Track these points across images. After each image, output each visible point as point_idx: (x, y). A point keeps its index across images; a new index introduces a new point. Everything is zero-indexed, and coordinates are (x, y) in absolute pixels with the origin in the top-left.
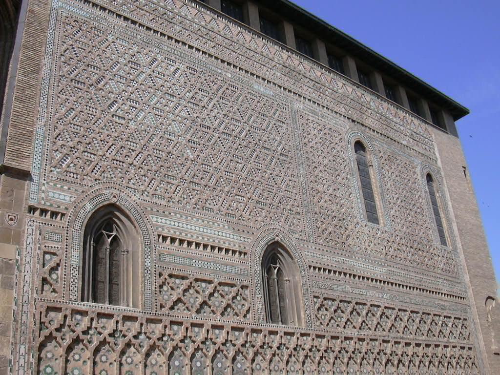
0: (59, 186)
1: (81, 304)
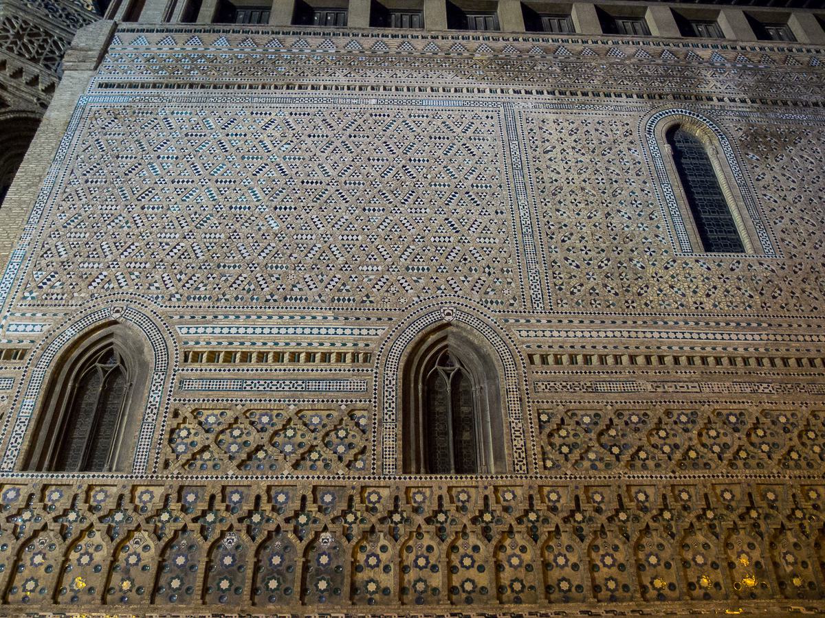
0: (28, 315)
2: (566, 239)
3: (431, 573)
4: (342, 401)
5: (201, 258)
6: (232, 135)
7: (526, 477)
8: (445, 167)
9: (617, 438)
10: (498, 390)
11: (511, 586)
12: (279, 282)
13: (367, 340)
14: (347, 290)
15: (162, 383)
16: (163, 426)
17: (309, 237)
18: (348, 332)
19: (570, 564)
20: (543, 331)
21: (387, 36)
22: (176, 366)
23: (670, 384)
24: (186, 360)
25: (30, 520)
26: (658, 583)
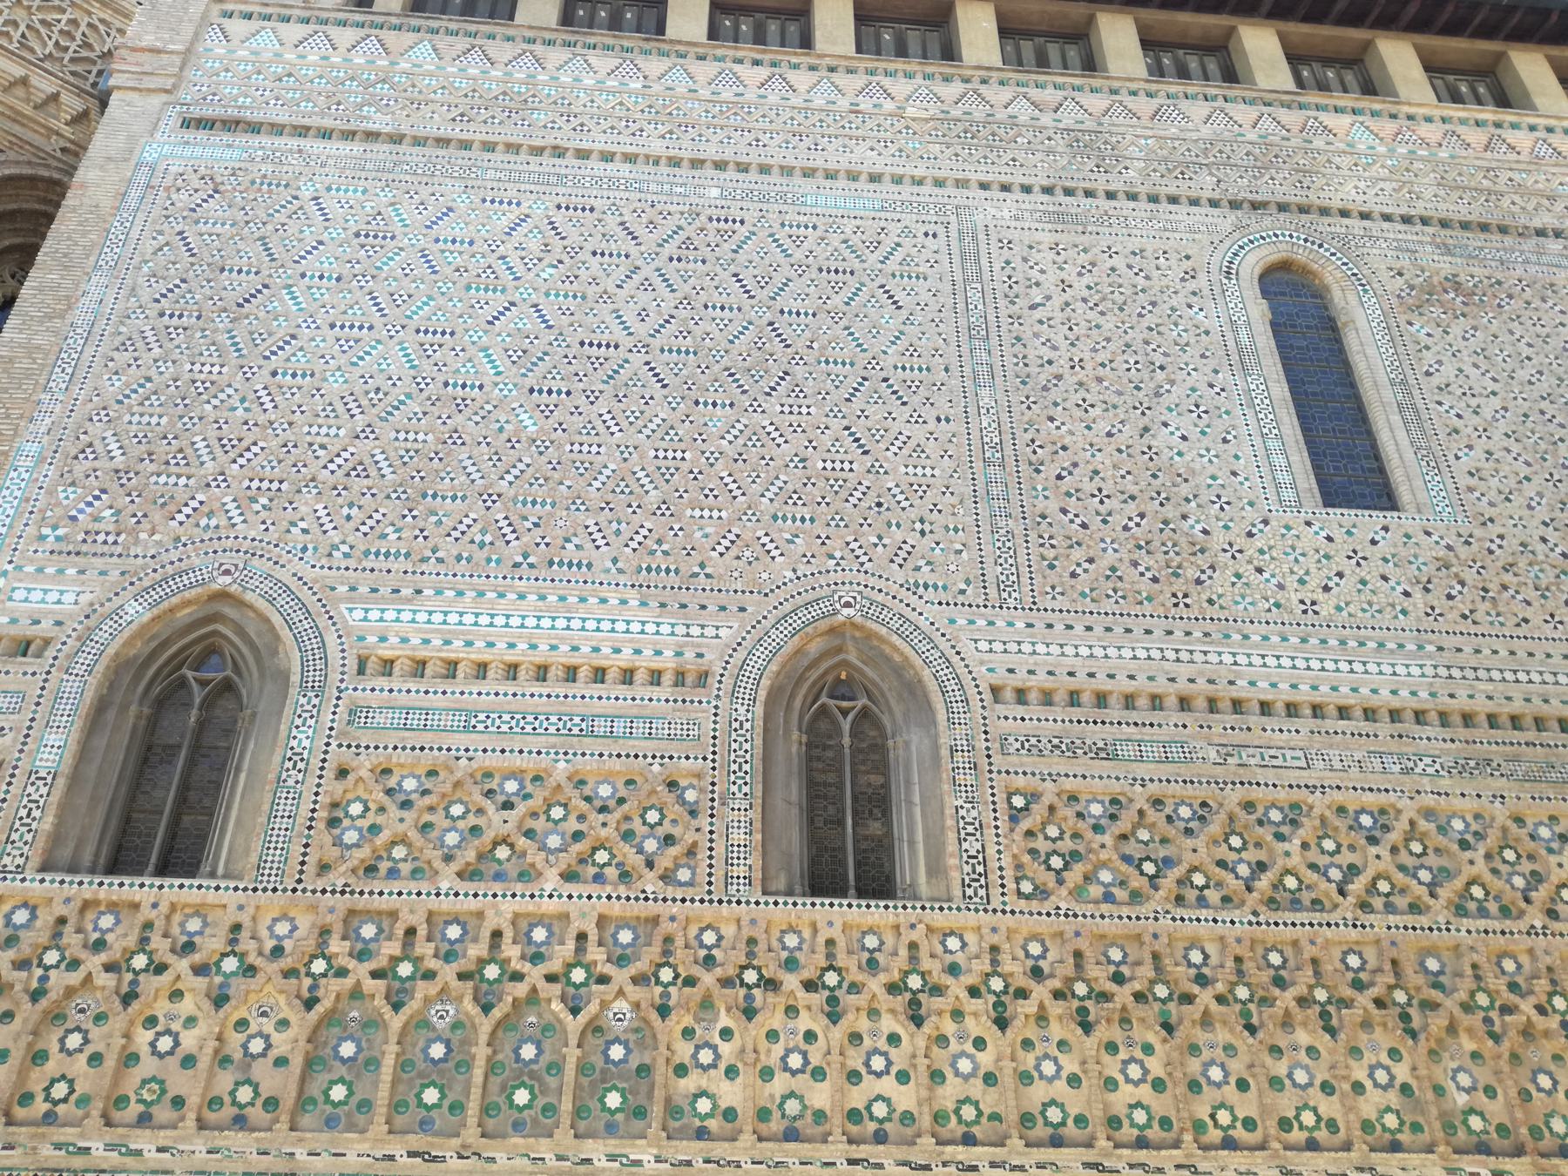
0: (50, 570)
1: (33, 880)
2: (1064, 473)
3: (811, 1082)
4: (654, 757)
5: (390, 477)
6: (445, 241)
7: (986, 911)
8: (847, 328)
10: (936, 747)
11: (957, 1111)
12: (538, 532)
13: (699, 646)
14: (665, 553)
15: (315, 712)
16: (317, 794)
17: (594, 449)
18: (665, 629)
19: (1064, 1074)
20: (1019, 643)
21: (740, 61)
22: (342, 681)
23: (1251, 751)
24: (361, 671)
25: (57, 967)
26: (1224, 1117)
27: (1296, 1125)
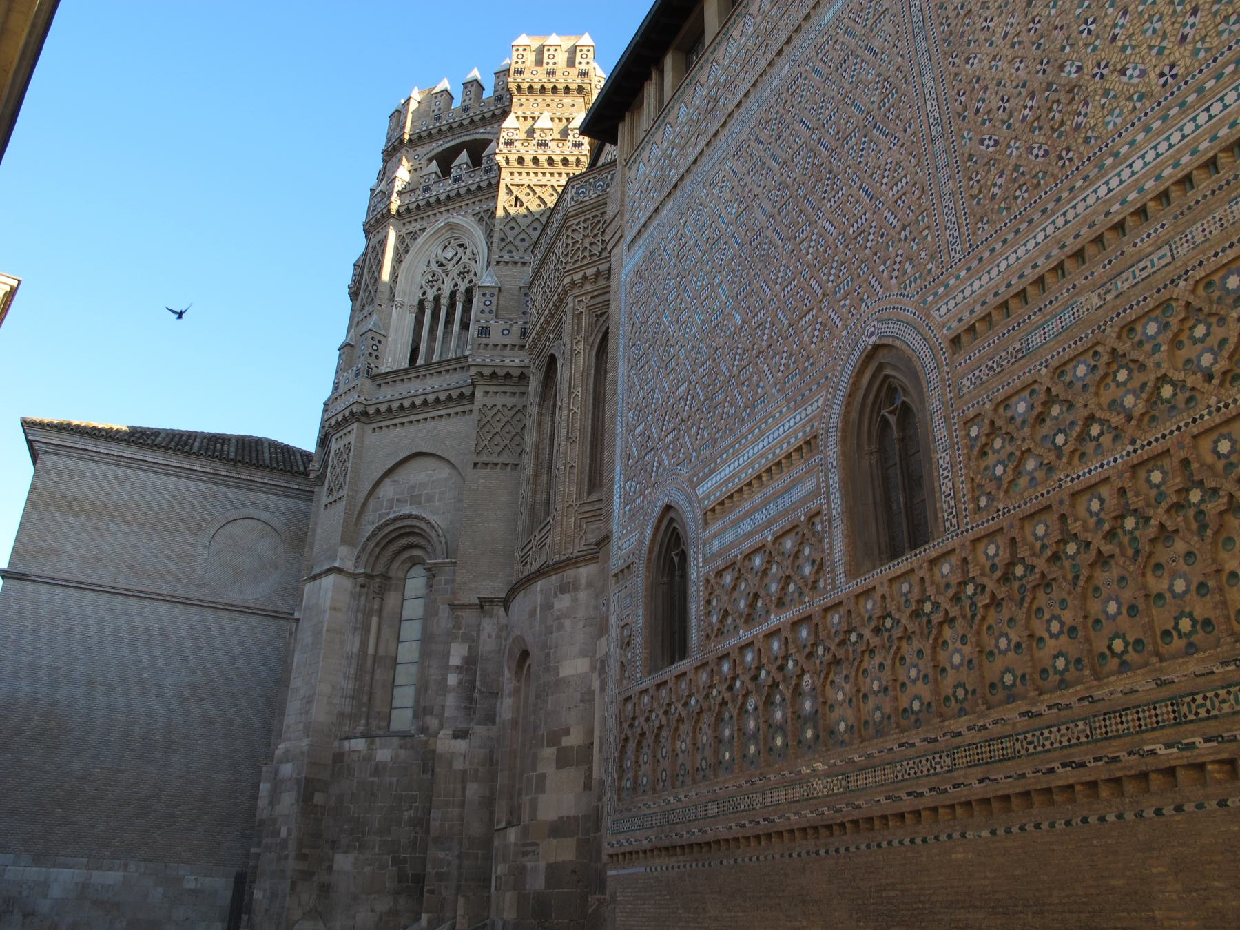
7: (957, 535)
9: (1060, 417)
27: (1175, 634)
